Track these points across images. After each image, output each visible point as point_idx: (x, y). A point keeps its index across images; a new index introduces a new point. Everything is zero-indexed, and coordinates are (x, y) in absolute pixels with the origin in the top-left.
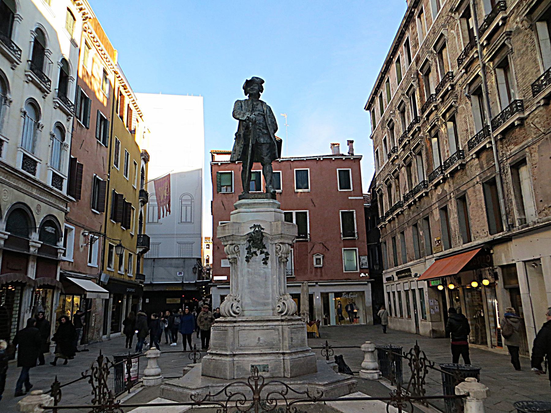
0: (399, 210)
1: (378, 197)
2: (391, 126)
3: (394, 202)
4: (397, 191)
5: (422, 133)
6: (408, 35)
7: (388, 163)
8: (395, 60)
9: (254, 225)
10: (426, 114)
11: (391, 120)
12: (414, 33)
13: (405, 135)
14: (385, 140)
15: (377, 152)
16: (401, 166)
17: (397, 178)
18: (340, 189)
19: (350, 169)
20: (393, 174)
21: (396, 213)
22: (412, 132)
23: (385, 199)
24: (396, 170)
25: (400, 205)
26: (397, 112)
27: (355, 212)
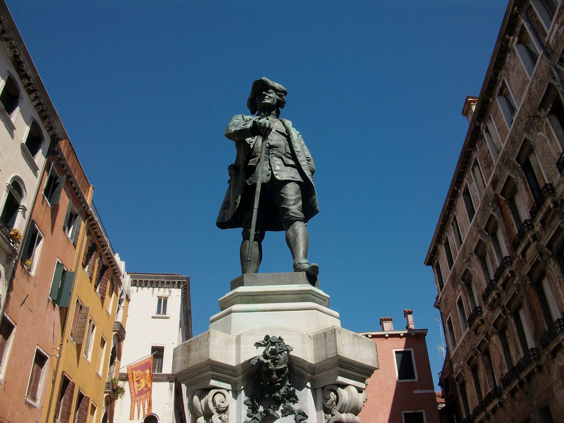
0: (496, 402)
1: (458, 389)
2: (467, 280)
3: (486, 390)
4: (488, 373)
5: (517, 278)
6: (475, 155)
7: (468, 333)
8: (461, 191)
9: (267, 337)
10: (520, 250)
12: (484, 151)
13: (491, 286)
15: (450, 322)
16: (490, 333)
17: (487, 353)
19: (412, 350)
20: (478, 348)
21: (491, 407)
22: (501, 281)
23: (470, 389)
25: (497, 393)
26: (474, 258)
27: (424, 414)
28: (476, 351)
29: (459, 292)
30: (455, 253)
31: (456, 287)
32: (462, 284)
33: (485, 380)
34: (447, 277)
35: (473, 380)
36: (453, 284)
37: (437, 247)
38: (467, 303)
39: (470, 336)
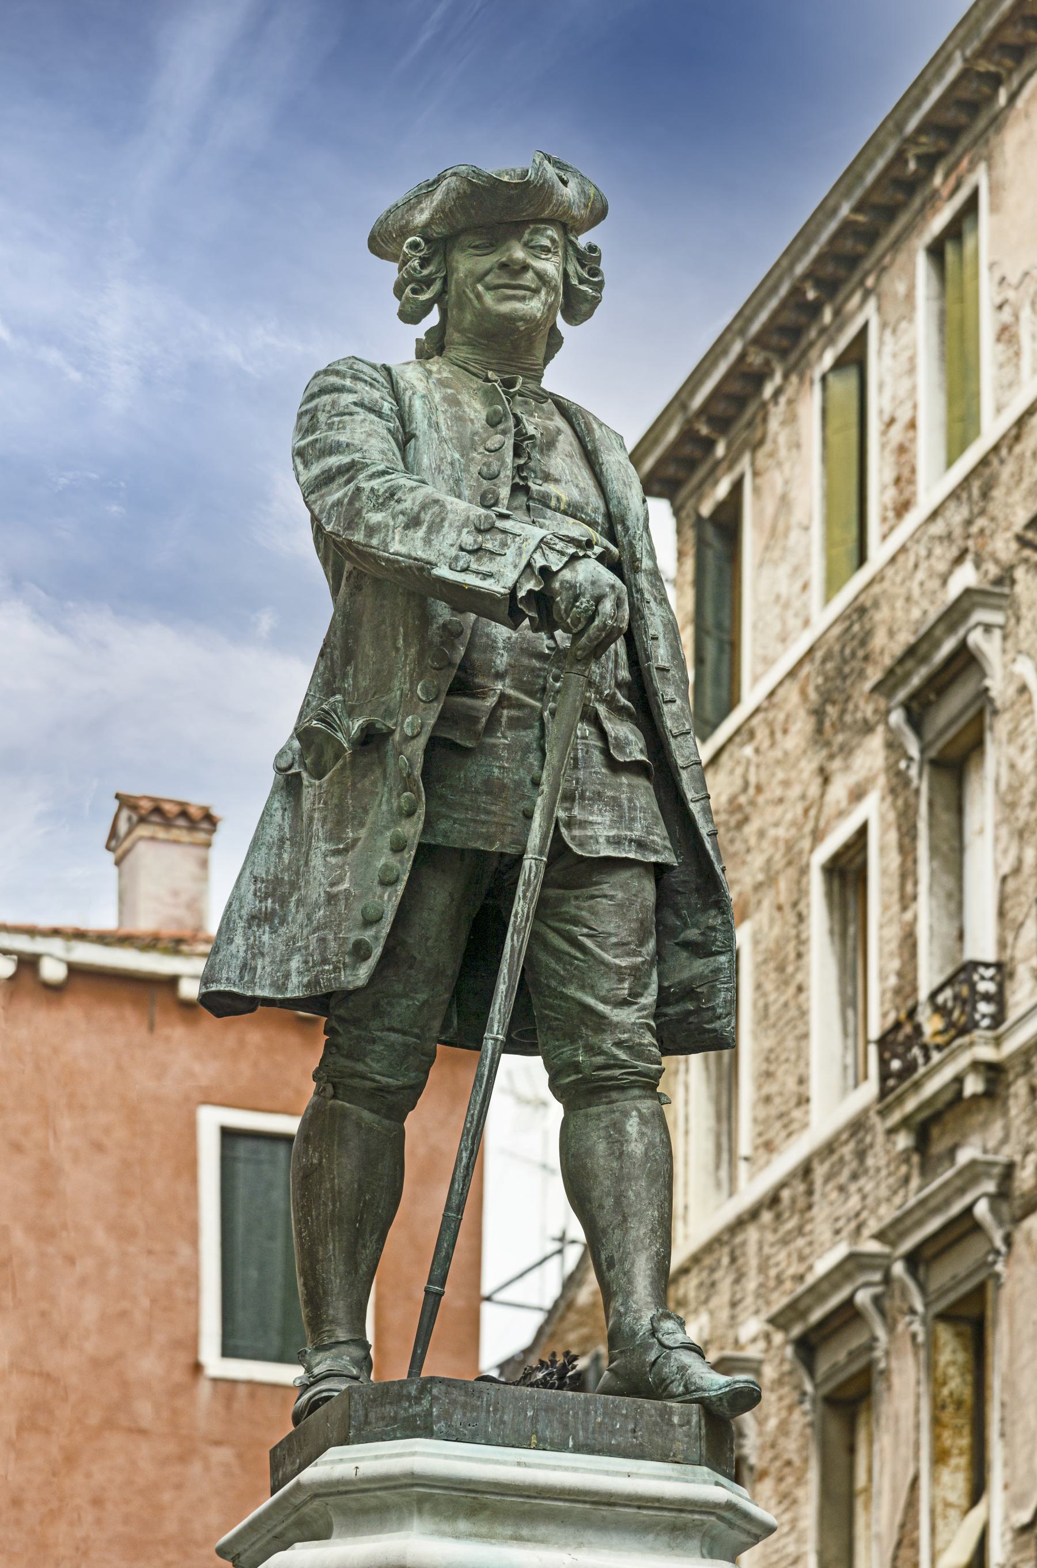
4: (940, 1457)
11: (965, 659)
14: (847, 872)
18: (228, 1351)
20: (913, 1260)
24: (965, 1225)
28: (887, 1279)
29: (857, 795)
30: (904, 480)
31: (847, 751)
32: (893, 745)
33: (912, 1503)
34: (784, 639)
35: (813, 1475)
36: (818, 713)
37: (759, 378)
38: (907, 900)
39: (861, 1155)
